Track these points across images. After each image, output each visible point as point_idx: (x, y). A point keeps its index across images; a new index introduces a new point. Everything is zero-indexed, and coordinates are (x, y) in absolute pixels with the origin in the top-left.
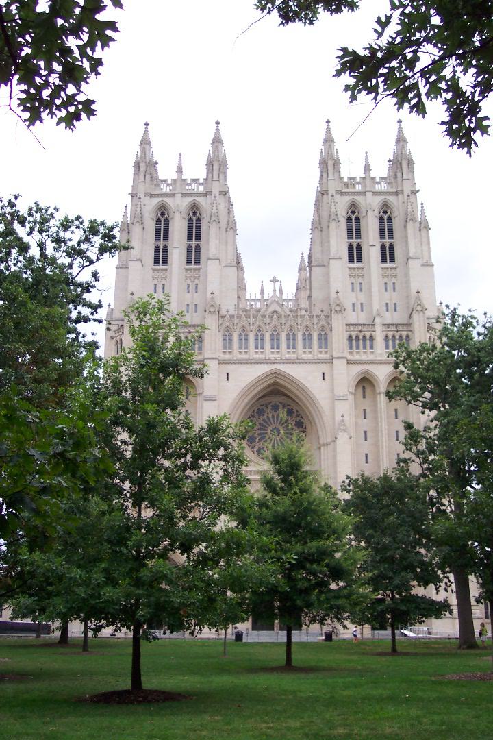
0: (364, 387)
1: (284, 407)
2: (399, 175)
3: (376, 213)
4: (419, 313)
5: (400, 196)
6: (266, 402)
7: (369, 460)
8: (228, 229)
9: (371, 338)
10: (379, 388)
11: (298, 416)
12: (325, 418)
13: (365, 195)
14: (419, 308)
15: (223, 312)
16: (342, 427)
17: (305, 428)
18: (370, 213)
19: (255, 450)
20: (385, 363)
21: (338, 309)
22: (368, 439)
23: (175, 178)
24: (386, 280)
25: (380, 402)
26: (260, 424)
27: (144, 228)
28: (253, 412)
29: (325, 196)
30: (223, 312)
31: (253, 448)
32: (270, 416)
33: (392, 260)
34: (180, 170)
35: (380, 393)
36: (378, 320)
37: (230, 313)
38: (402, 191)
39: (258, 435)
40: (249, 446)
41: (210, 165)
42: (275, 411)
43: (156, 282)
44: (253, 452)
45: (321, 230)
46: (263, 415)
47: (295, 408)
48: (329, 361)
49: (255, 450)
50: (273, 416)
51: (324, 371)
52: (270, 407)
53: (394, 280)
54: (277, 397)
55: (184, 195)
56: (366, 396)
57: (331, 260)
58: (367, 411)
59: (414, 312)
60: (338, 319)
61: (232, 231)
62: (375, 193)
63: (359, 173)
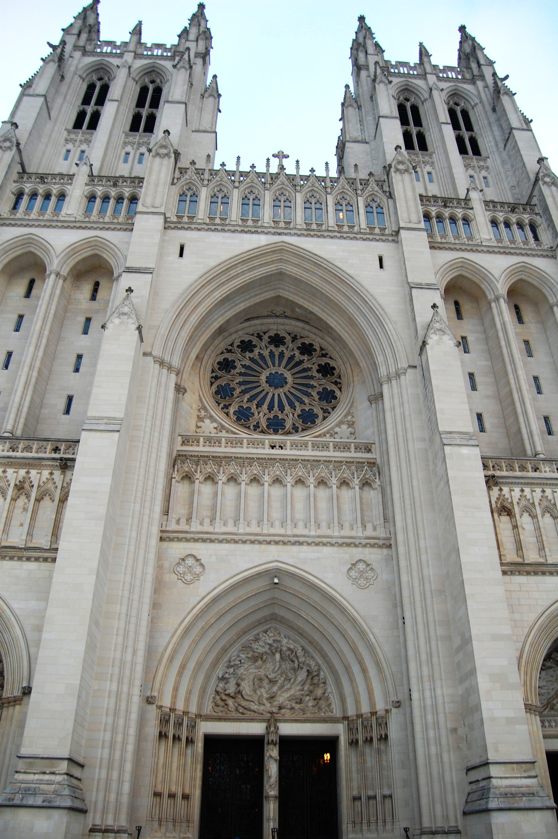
0: (457, 303)
1: (294, 339)
2: (474, 66)
3: (444, 96)
4: (550, 186)
5: (480, 84)
6: (259, 328)
7: (487, 425)
8: (206, 95)
9: (466, 221)
10: (493, 289)
11: (324, 355)
12: (389, 327)
13: (426, 79)
14: (547, 179)
15: (184, 163)
16: (437, 325)
17: (340, 377)
18: (435, 93)
19: (232, 410)
20: (499, 253)
21: (401, 167)
22: (479, 387)
23: (127, 40)
24: (471, 172)
25: (501, 313)
26: (244, 366)
27: (63, 77)
28: (232, 345)
29: (363, 73)
30: (184, 163)
31: (226, 407)
32: (266, 353)
33: (477, 151)
34: (137, 31)
35: (497, 299)
36: (474, 195)
37: (197, 166)
38: (482, 77)
39: (240, 384)
40: (219, 404)
41: (184, 34)
42: (277, 346)
43: (70, 146)
44: (227, 414)
45: (359, 107)
46: (251, 351)
47: (317, 340)
48: (391, 238)
49: (232, 410)
50: (272, 354)
51: (381, 253)
52: (266, 338)
53: (484, 173)
54: (280, 320)
55: (137, 56)
56: (464, 314)
57: (381, 119)
58: (469, 339)
59: (540, 183)
60: (403, 180)
61: (211, 99)
62: (439, 79)
63: (414, 59)
